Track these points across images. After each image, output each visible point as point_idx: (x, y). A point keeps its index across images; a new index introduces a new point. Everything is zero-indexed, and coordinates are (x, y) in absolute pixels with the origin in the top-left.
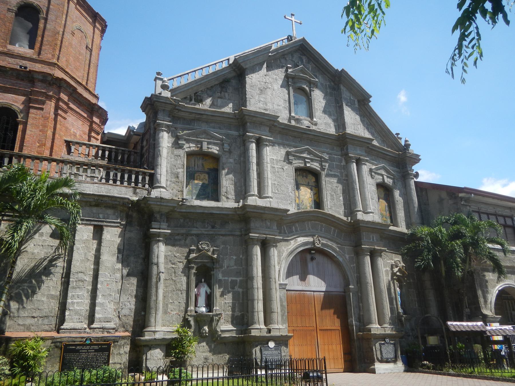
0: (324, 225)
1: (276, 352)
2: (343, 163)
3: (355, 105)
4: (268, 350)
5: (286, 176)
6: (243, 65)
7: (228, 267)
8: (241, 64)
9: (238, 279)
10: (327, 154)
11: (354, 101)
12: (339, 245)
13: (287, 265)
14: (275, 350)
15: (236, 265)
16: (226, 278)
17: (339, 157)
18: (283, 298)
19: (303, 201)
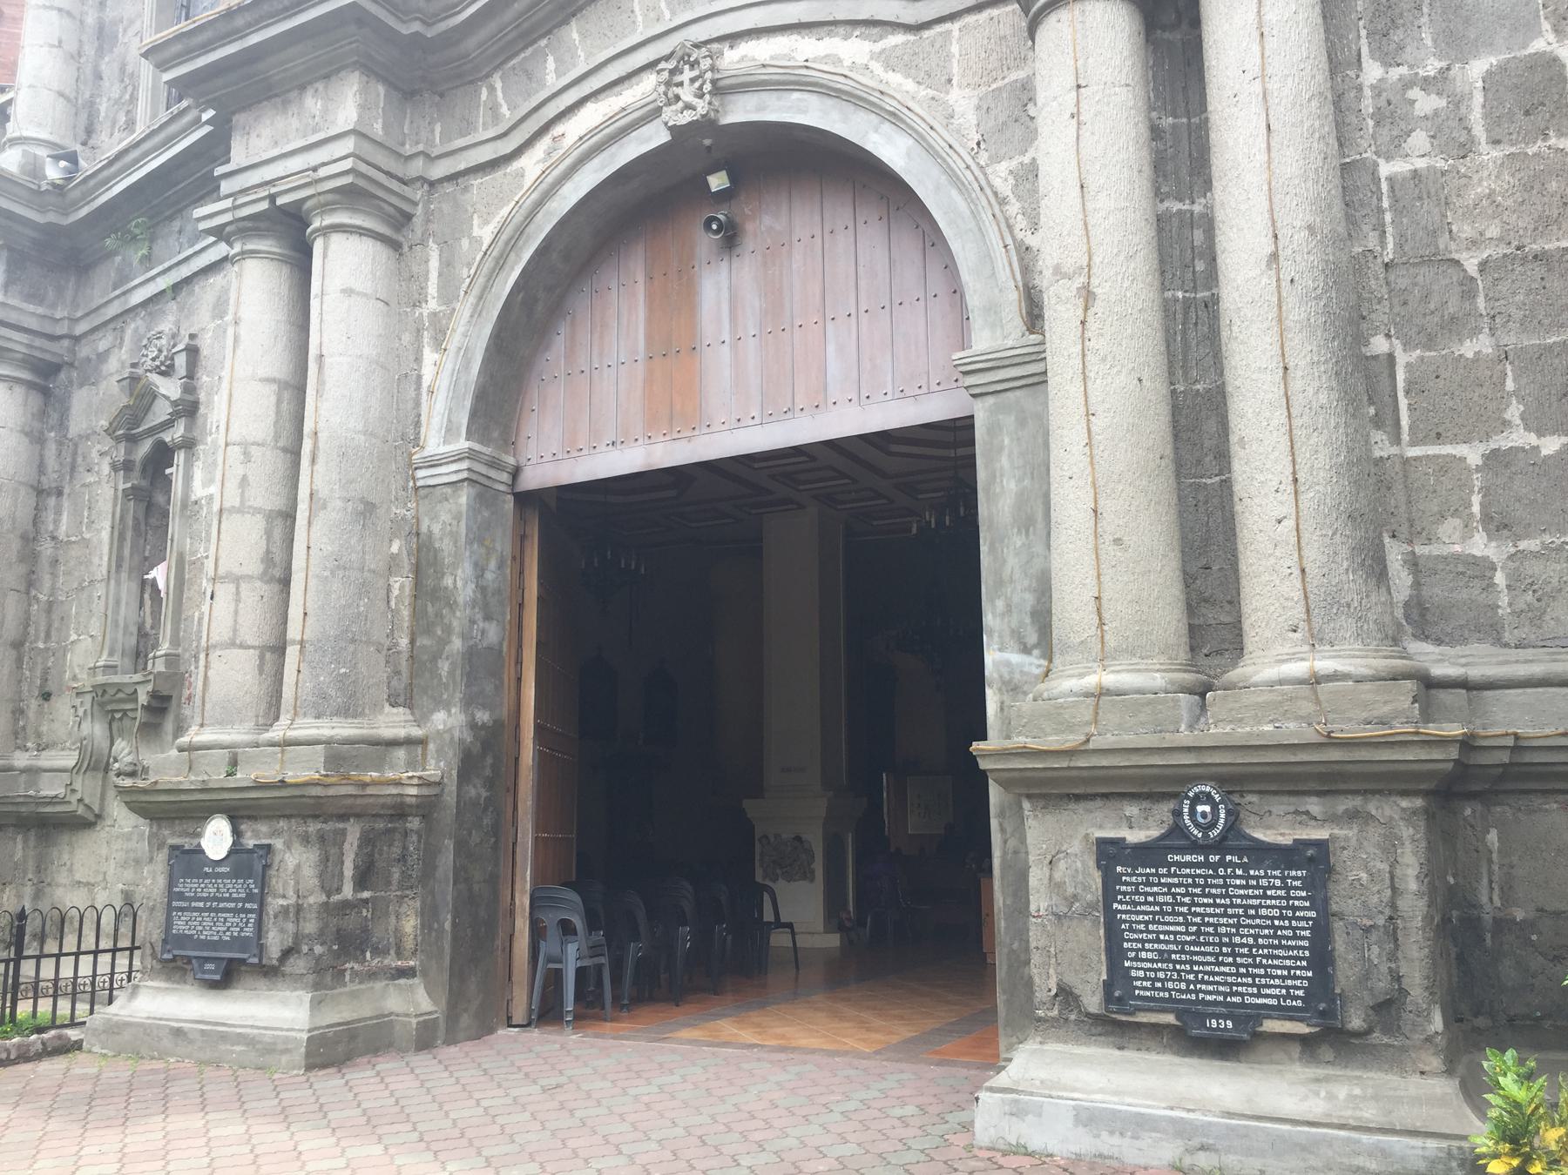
1: (236, 888)
12: (898, 39)
13: (488, 330)
14: (236, 874)
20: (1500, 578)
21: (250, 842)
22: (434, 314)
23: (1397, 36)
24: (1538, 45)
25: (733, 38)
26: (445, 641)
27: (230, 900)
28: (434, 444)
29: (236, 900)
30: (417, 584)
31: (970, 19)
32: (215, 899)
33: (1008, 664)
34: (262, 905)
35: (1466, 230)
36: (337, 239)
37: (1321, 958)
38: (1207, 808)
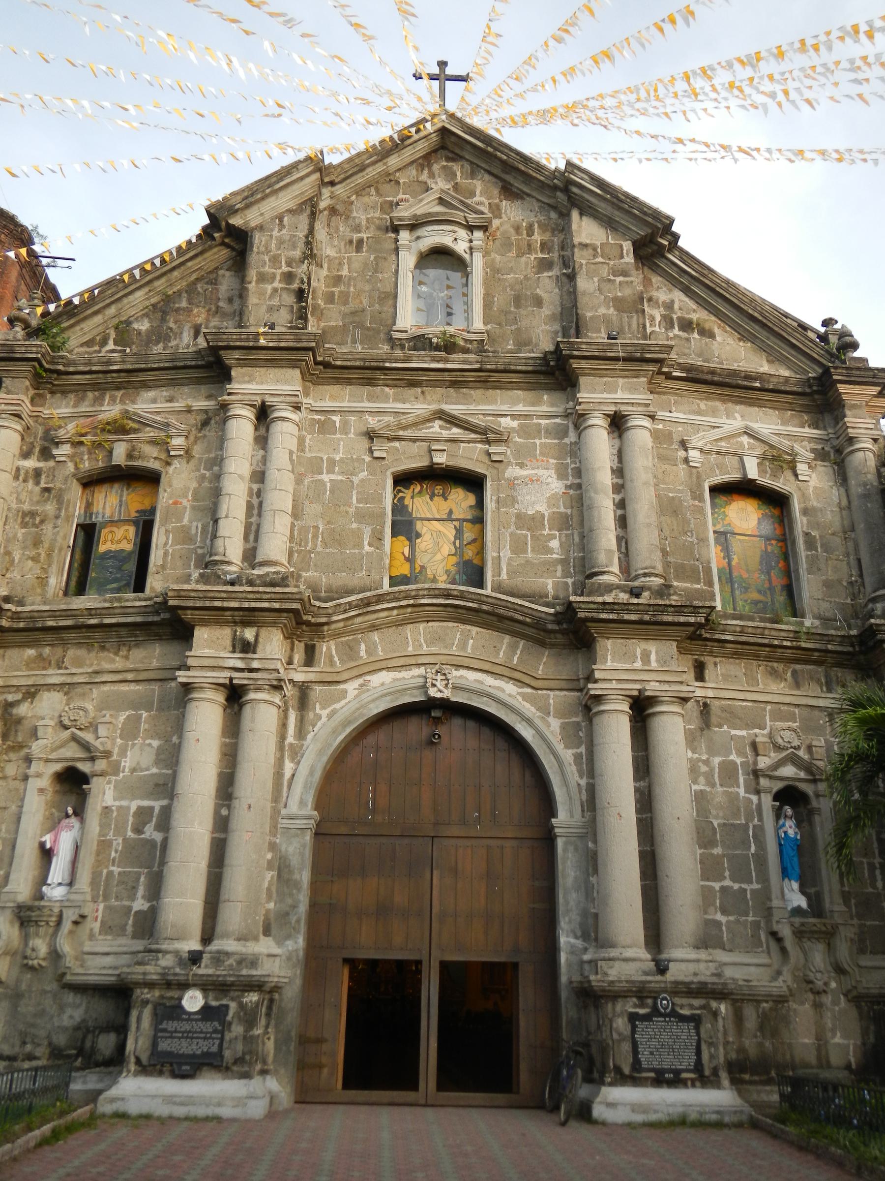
0: (474, 630)
1: (208, 1027)
2: (572, 437)
3: (622, 257)
4: (179, 1019)
5: (359, 501)
6: (236, 221)
7: (133, 770)
8: (231, 222)
9: (157, 805)
10: (514, 417)
11: (621, 246)
12: (529, 690)
13: (325, 759)
15: (157, 762)
16: (124, 803)
17: (558, 420)
18: (295, 861)
19: (423, 567)
20: (724, 928)
21: (214, 1003)
22: (291, 745)
23: (696, 743)
24: (732, 757)
25: (458, 667)
26: (294, 907)
27: (201, 1032)
28: (293, 807)
29: (207, 1033)
30: (279, 876)
31: (557, 693)
32: (190, 1032)
33: (569, 942)
34: (223, 1036)
35: (714, 812)
36: (263, 706)
37: (698, 1052)
38: (665, 1002)
